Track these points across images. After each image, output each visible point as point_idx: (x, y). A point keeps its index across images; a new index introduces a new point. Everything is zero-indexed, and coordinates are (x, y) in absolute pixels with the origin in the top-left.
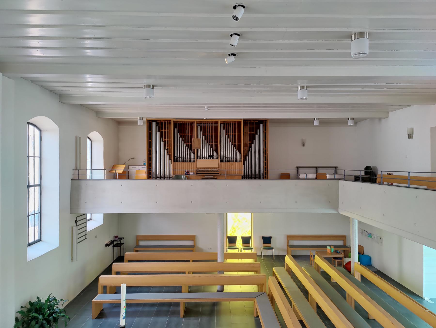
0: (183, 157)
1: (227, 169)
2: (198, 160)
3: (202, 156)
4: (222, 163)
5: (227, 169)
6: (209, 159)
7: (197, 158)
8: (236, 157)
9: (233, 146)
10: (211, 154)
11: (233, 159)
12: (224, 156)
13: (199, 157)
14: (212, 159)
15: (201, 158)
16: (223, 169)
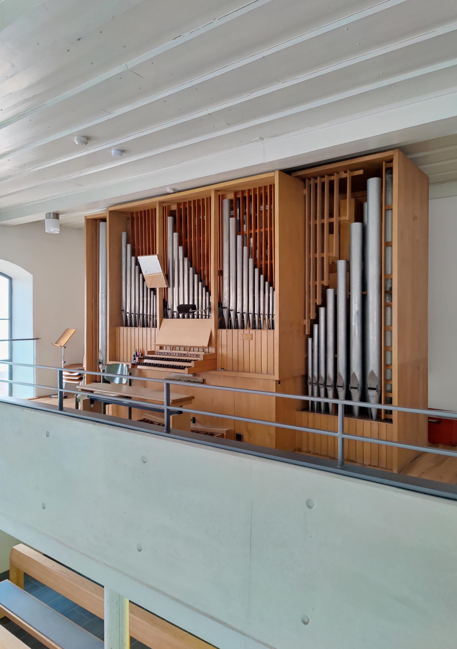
0: (137, 312)
1: (235, 352)
2: (165, 320)
3: (240, 311)
4: (224, 332)
5: (235, 352)
6: (178, 317)
7: (165, 315)
8: (256, 312)
9: (257, 270)
10: (191, 303)
11: (256, 316)
12: (232, 307)
13: (169, 313)
14: (193, 317)
15: (200, 316)
16: (224, 351)
